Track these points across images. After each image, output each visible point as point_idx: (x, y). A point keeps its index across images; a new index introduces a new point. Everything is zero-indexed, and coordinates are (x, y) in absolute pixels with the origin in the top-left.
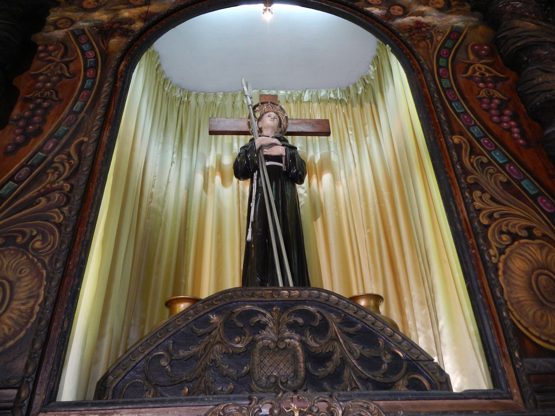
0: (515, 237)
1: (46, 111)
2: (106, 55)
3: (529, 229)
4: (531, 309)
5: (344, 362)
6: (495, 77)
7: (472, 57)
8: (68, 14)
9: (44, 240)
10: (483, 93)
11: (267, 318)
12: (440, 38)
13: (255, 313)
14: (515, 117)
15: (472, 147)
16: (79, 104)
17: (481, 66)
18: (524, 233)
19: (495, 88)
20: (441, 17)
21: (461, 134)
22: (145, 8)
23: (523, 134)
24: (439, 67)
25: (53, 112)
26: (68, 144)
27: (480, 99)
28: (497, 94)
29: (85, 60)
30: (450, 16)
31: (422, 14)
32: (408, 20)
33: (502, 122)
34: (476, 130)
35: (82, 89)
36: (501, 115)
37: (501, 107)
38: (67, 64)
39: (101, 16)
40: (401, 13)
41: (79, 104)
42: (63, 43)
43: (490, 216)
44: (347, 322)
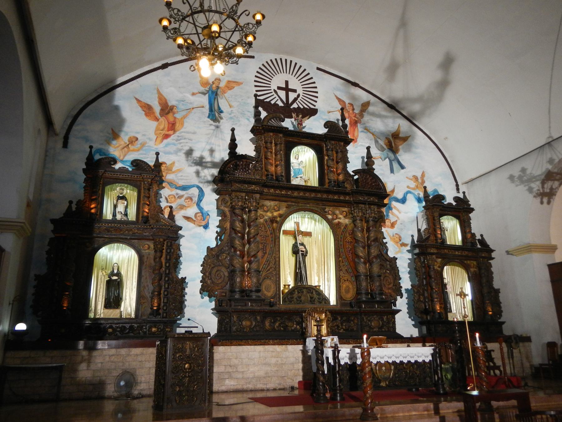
0: (345, 281)
1: (266, 246)
2: (274, 230)
3: (348, 279)
4: (344, 293)
5: (315, 298)
6: (351, 242)
7: (348, 235)
8: (262, 213)
9: (273, 278)
10: (347, 247)
11: (305, 290)
12: (342, 228)
13: (302, 289)
14: (352, 254)
15: (343, 261)
16: (271, 245)
17: (349, 238)
18: (346, 280)
19: (350, 245)
20: (344, 220)
21: (341, 258)
22: (279, 212)
23: (352, 258)
24: (341, 238)
25: (267, 247)
26: (272, 257)
27: (347, 248)
28: (350, 247)
29: (270, 231)
30: (346, 220)
31: (340, 218)
32: (336, 221)
33: (349, 254)
34: (344, 257)
35: (271, 241)
36: (350, 252)
37: (349, 251)
38: (266, 232)
39: (269, 214)
40: (335, 218)
41: (271, 245)
42: (263, 224)
43: (342, 277)
44: (316, 291)
